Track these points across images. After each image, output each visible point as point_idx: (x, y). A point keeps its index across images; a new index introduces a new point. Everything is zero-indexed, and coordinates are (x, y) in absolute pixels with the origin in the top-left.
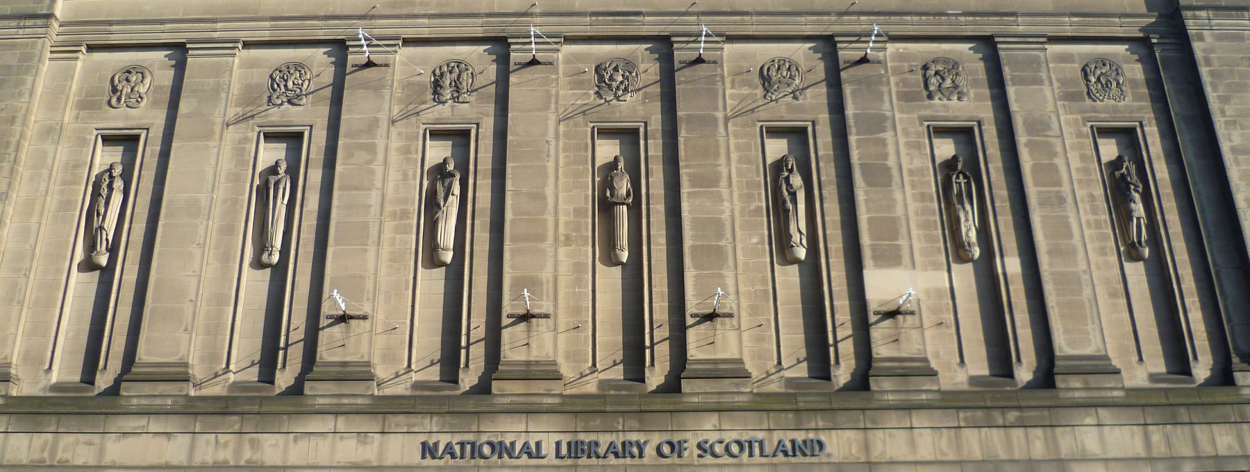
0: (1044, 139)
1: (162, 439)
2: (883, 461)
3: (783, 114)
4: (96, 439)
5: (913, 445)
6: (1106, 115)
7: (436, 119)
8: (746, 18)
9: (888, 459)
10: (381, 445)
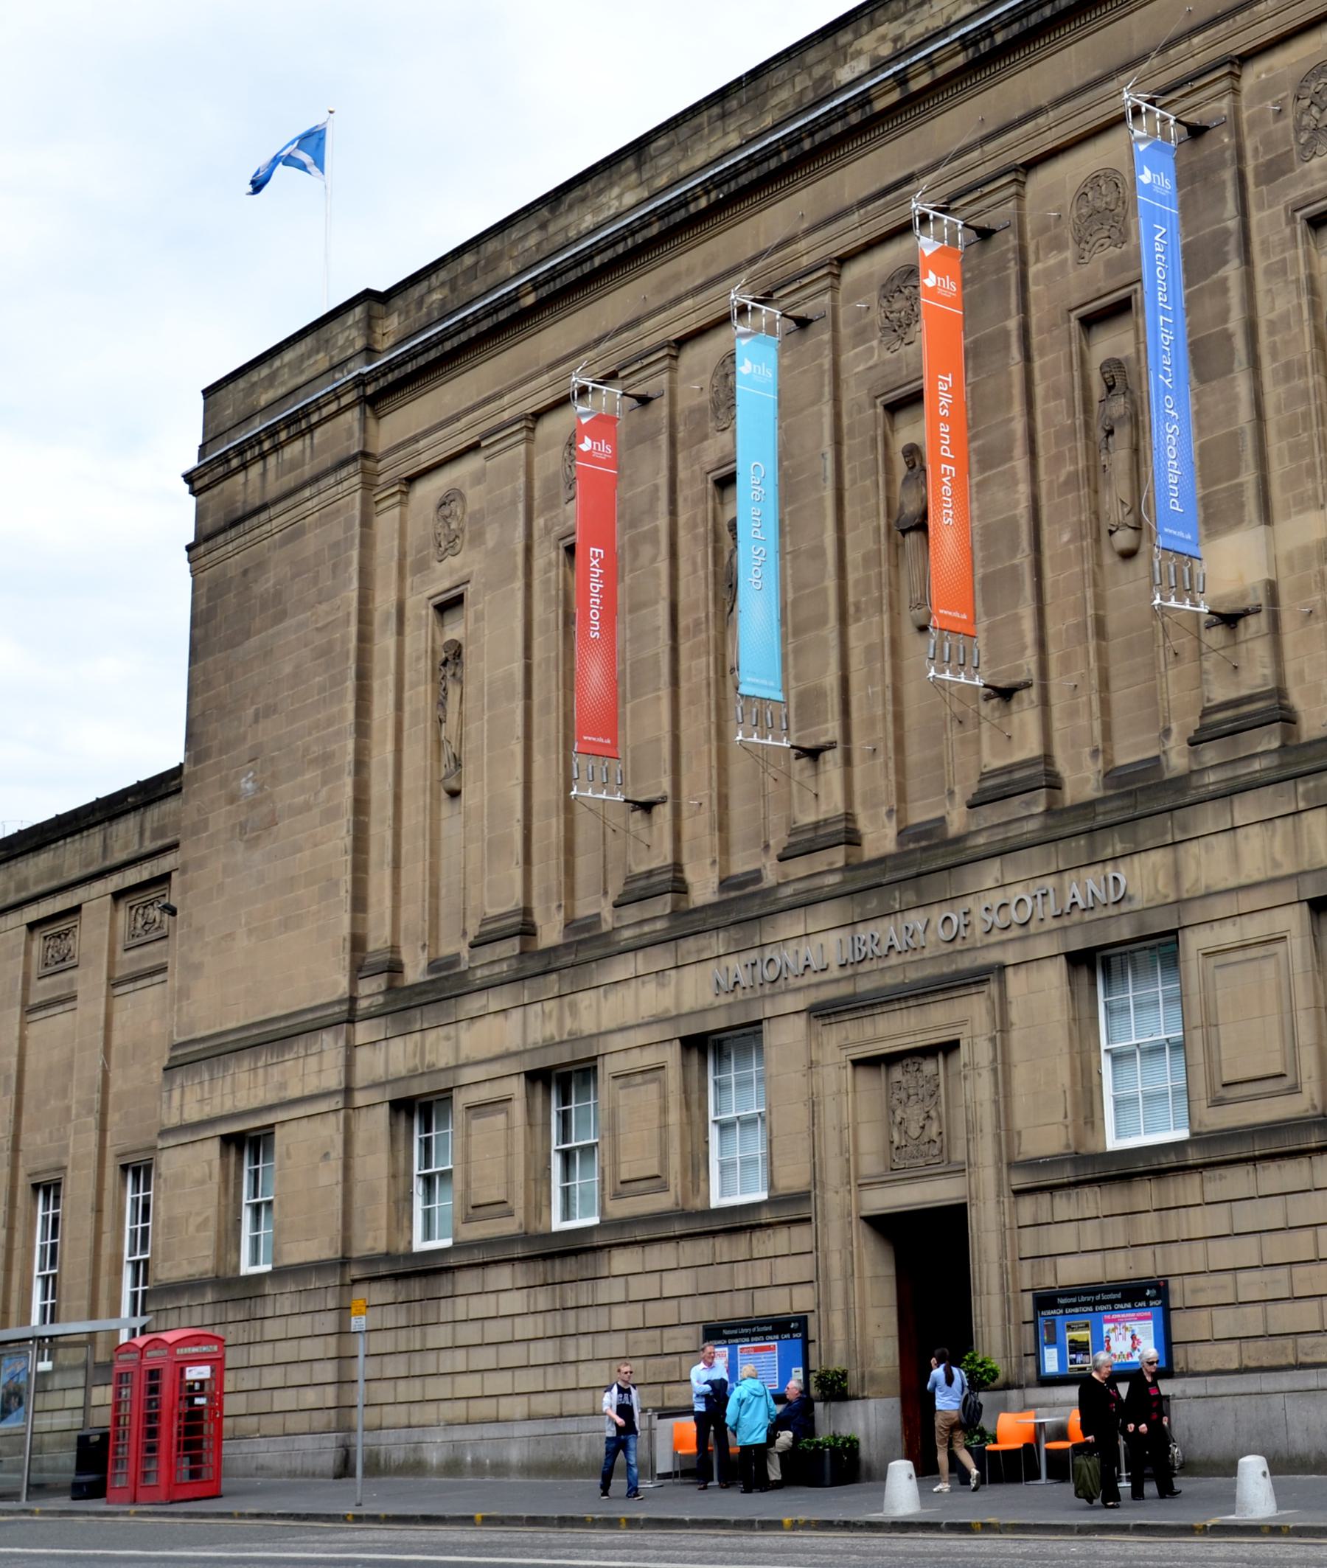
1: (501, 1017)
2: (1198, 894)
3: (1101, 284)
4: (451, 1029)
5: (1236, 856)
7: (719, 460)
8: (1041, 120)
9: (1202, 891)
10: (678, 984)
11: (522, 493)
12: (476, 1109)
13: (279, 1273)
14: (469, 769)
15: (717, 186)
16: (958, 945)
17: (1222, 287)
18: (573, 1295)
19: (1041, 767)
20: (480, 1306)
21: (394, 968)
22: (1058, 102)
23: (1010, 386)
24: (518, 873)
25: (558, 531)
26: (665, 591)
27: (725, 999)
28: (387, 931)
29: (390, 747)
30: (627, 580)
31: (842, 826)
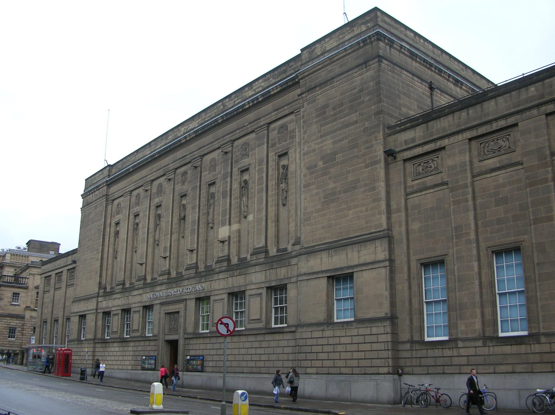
0: (262, 167)
6: (281, 149)
11: (129, 205)
12: (114, 315)
13: (86, 340)
14: (118, 254)
15: (159, 153)
16: (181, 295)
17: (227, 182)
18: (126, 349)
19: (195, 265)
20: (113, 349)
21: (105, 288)
22: (208, 145)
23: (197, 195)
24: (123, 274)
25: (134, 212)
26: (147, 225)
27: (149, 300)
28: (105, 282)
29: (107, 248)
30: (142, 223)
31: (123, 282)
